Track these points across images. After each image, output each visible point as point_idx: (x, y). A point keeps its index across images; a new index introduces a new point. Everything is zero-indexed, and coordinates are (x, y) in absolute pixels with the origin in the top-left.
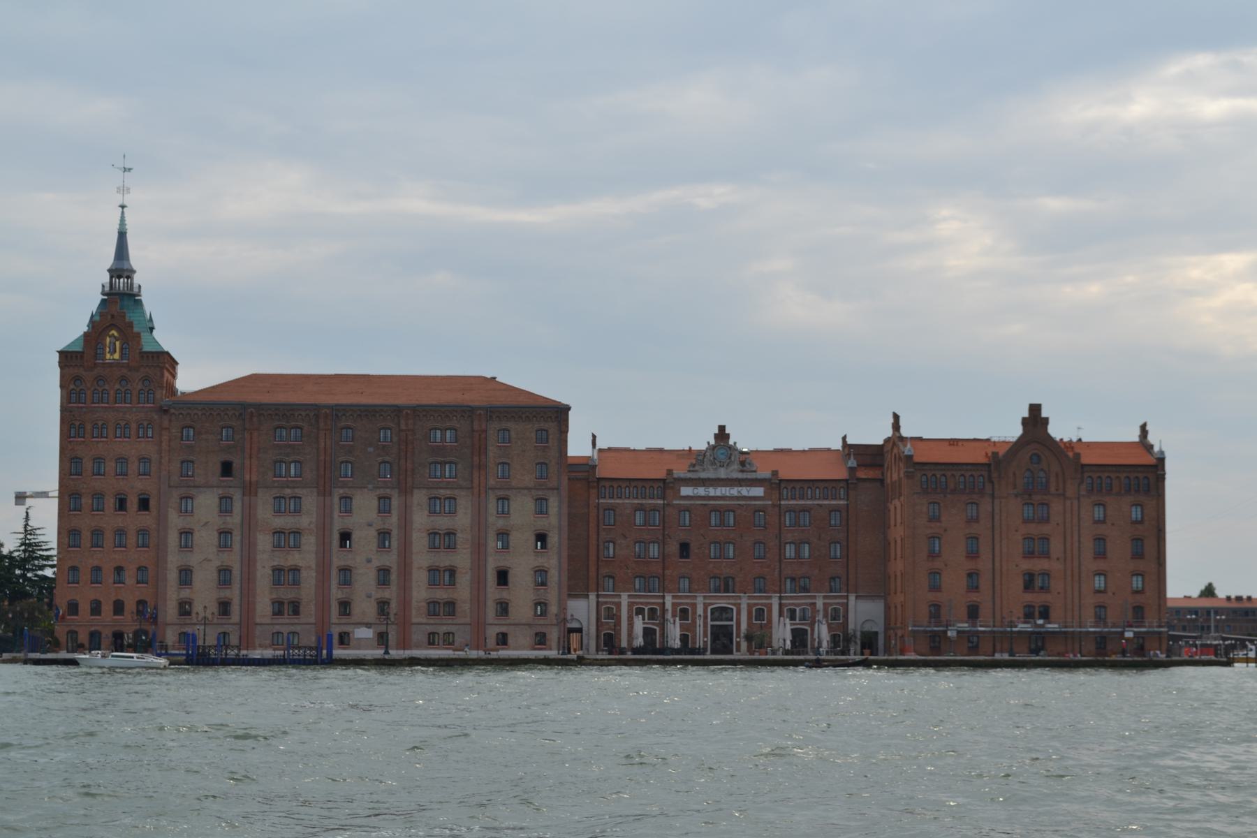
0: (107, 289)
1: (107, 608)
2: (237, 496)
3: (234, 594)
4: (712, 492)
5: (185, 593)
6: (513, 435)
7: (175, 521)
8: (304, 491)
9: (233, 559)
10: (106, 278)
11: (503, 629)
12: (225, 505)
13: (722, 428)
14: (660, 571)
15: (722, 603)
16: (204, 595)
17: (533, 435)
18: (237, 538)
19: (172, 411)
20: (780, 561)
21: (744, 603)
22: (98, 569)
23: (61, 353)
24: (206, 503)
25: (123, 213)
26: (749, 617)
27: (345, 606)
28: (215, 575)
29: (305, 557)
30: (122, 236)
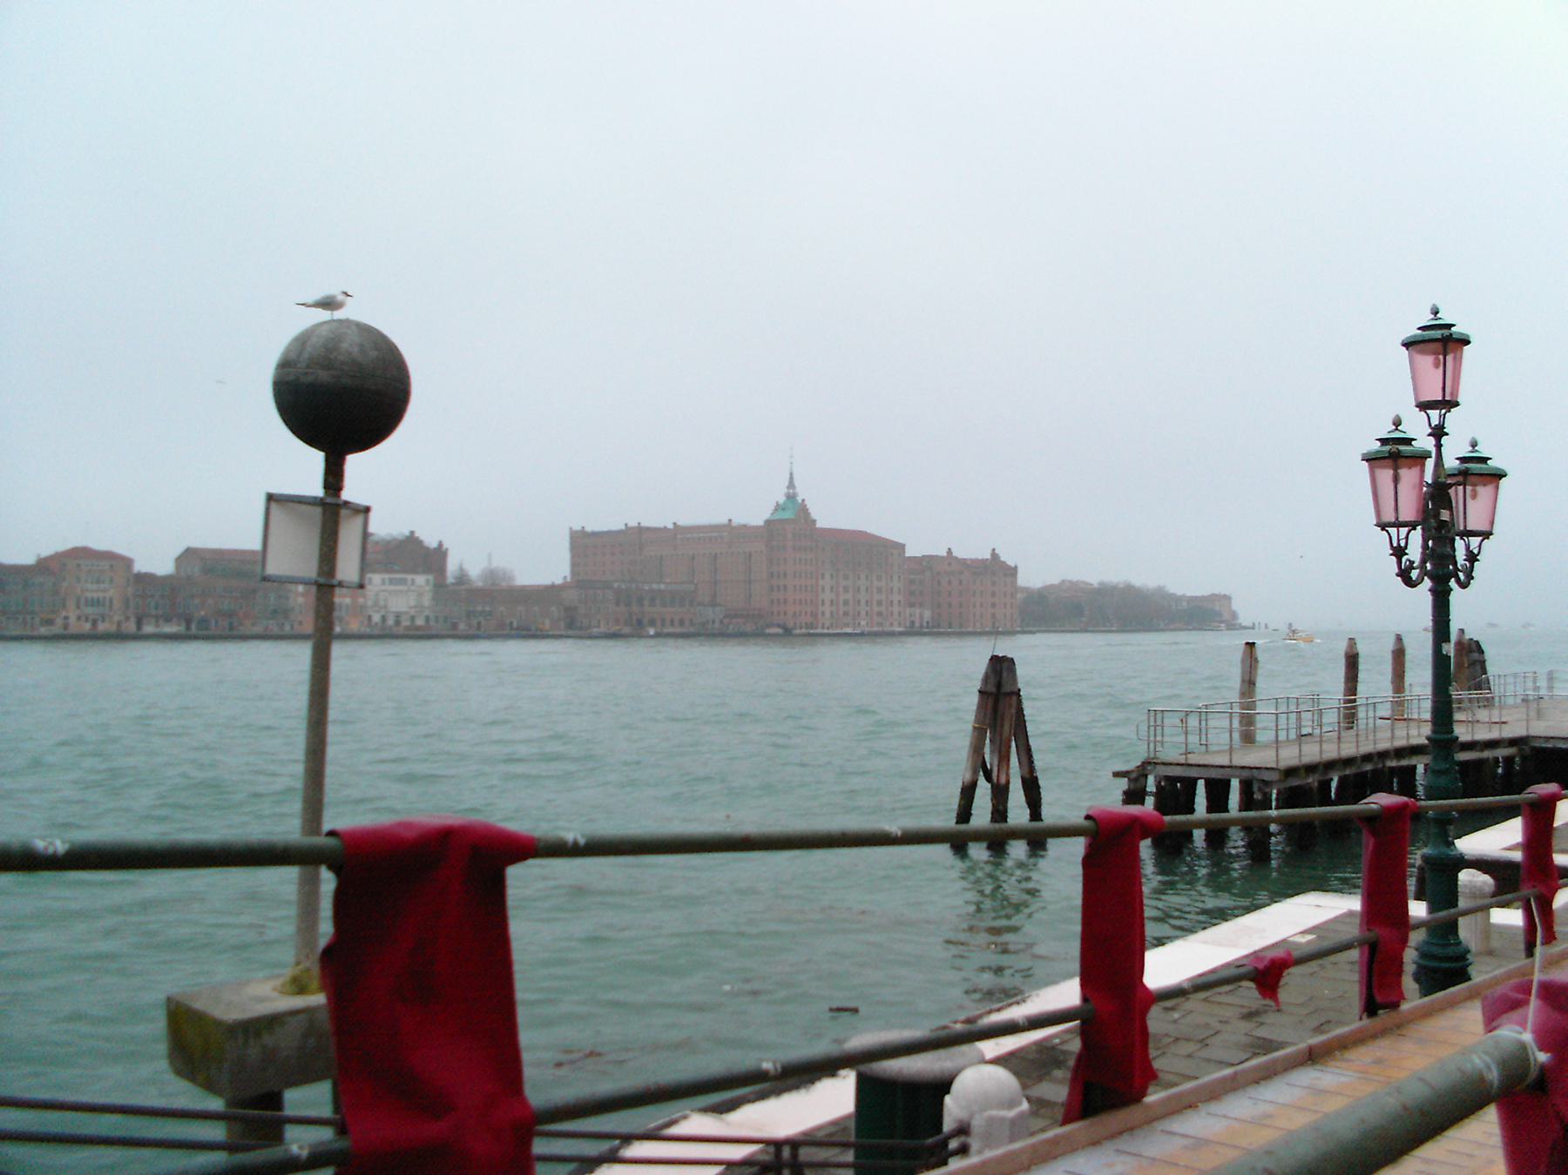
3: (834, 608)
7: (821, 582)
10: (786, 490)
24: (827, 576)
30: (791, 474)
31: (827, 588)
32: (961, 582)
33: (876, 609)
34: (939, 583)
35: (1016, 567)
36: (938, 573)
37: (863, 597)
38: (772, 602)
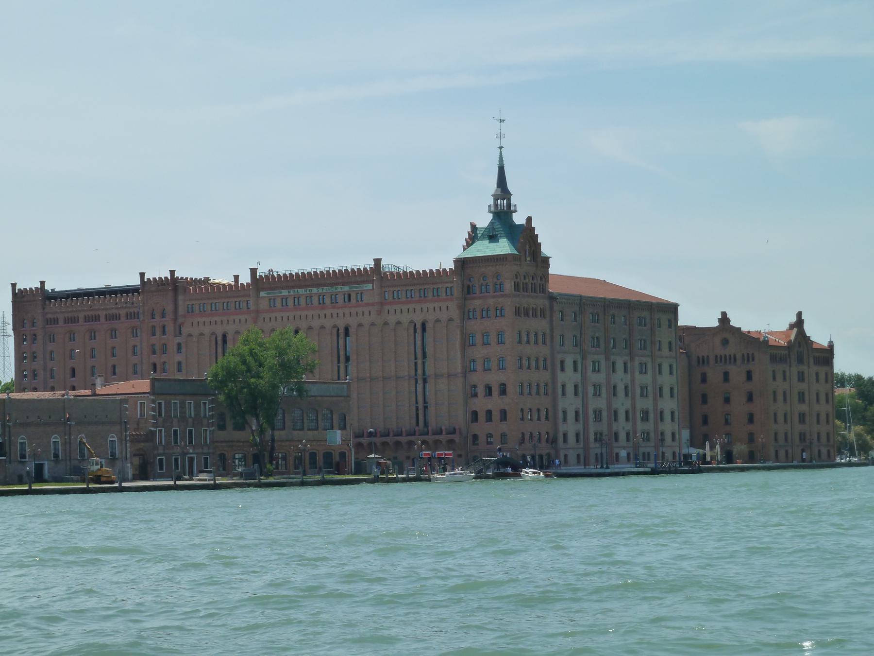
0: (492, 209)
3: (580, 427)
7: (561, 377)
25: (501, 152)
31: (570, 389)
32: (749, 376)
33: (640, 426)
34: (704, 380)
35: (831, 346)
36: (703, 361)
37: (622, 404)
38: (475, 414)
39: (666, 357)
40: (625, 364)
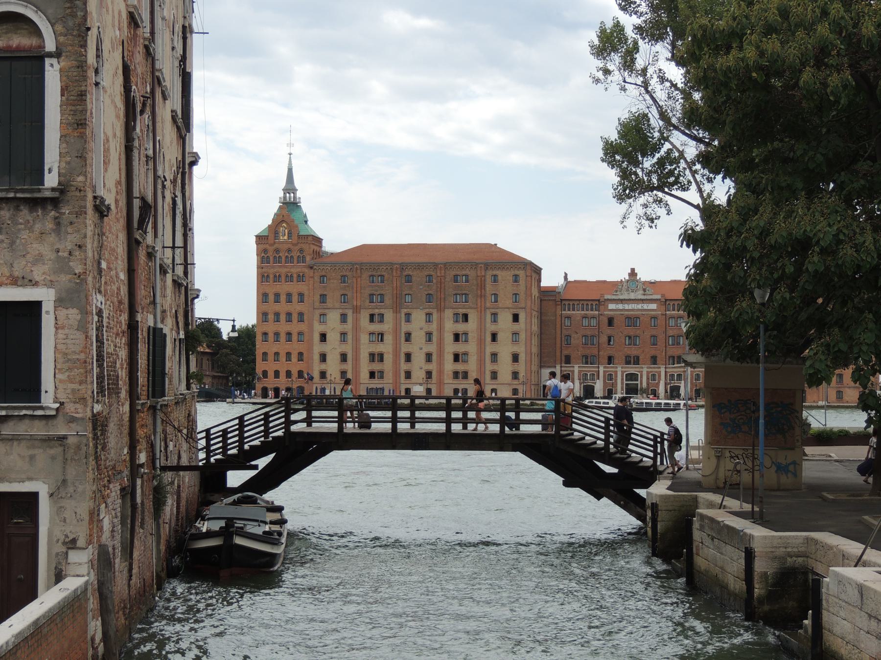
1: (283, 375)
2: (350, 314)
4: (627, 307)
5: (323, 367)
6: (500, 278)
8: (386, 310)
9: (348, 348)
10: (282, 195)
11: (494, 387)
12: (344, 318)
13: (633, 270)
14: (597, 353)
15: (632, 371)
16: (333, 367)
17: (511, 278)
18: (350, 337)
19: (315, 267)
20: (666, 347)
21: (645, 371)
22: (277, 354)
23: (257, 236)
24: (333, 317)
26: (648, 379)
27: (408, 375)
28: (339, 357)
29: (386, 347)
30: (290, 171)
37: (418, 348)
39: (508, 308)
40: (429, 315)
